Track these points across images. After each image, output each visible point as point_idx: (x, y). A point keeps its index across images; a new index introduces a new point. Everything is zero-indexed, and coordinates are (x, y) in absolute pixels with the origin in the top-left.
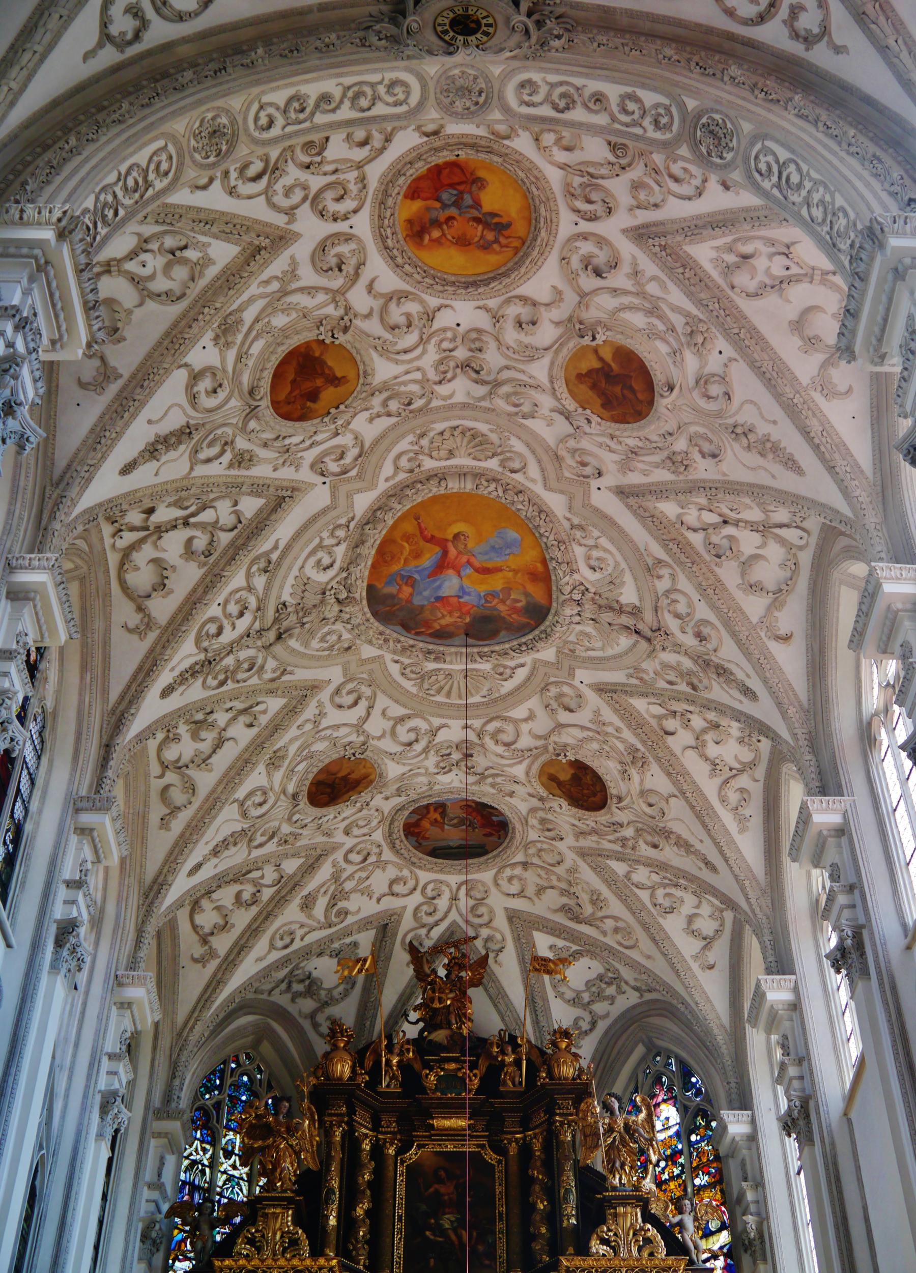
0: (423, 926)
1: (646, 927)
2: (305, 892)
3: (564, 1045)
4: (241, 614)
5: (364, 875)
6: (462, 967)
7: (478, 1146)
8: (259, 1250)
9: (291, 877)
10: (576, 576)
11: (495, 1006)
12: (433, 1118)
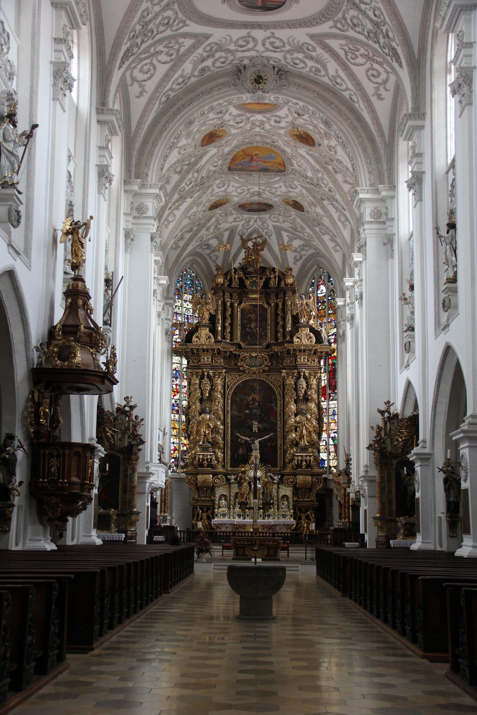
4: (191, 183)
6: (258, 246)
8: (199, 339)
10: (293, 167)
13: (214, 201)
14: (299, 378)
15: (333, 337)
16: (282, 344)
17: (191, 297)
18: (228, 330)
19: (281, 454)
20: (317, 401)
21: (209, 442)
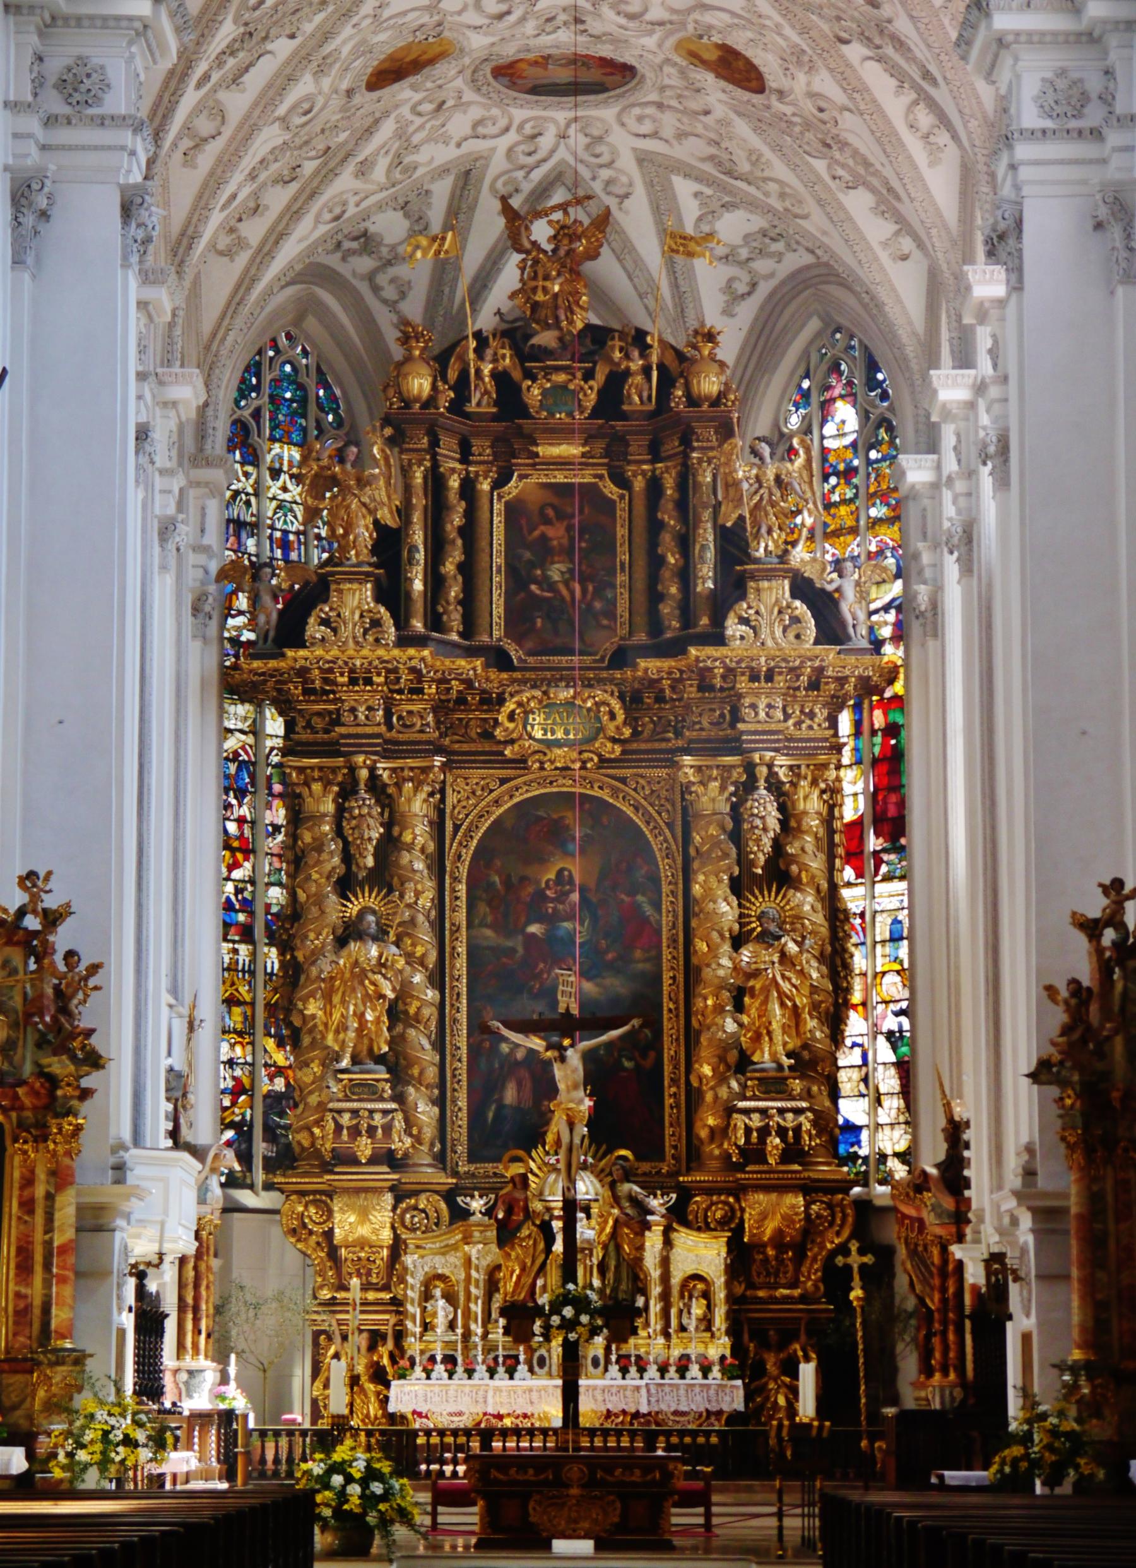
0: (522, 167)
1: (820, 202)
2: (360, 158)
3: (706, 353)
5: (438, 123)
6: (574, 237)
7: (595, 476)
8: (335, 631)
9: (341, 145)
11: (620, 260)
12: (537, 445)
13: (389, 50)
14: (749, 786)
15: (891, 617)
16: (676, 648)
17: (297, 456)
18: (454, 591)
20: (824, 885)
21: (380, 1059)
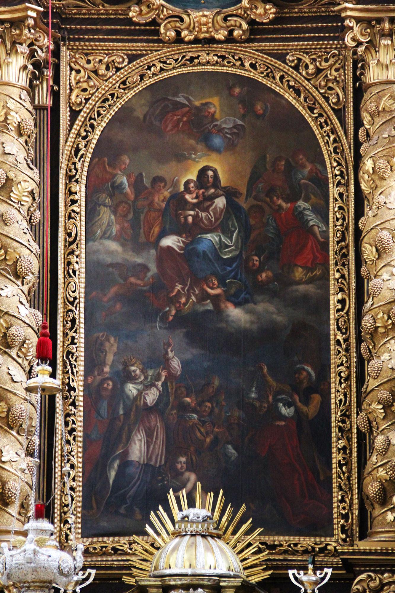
19: (348, 463)
